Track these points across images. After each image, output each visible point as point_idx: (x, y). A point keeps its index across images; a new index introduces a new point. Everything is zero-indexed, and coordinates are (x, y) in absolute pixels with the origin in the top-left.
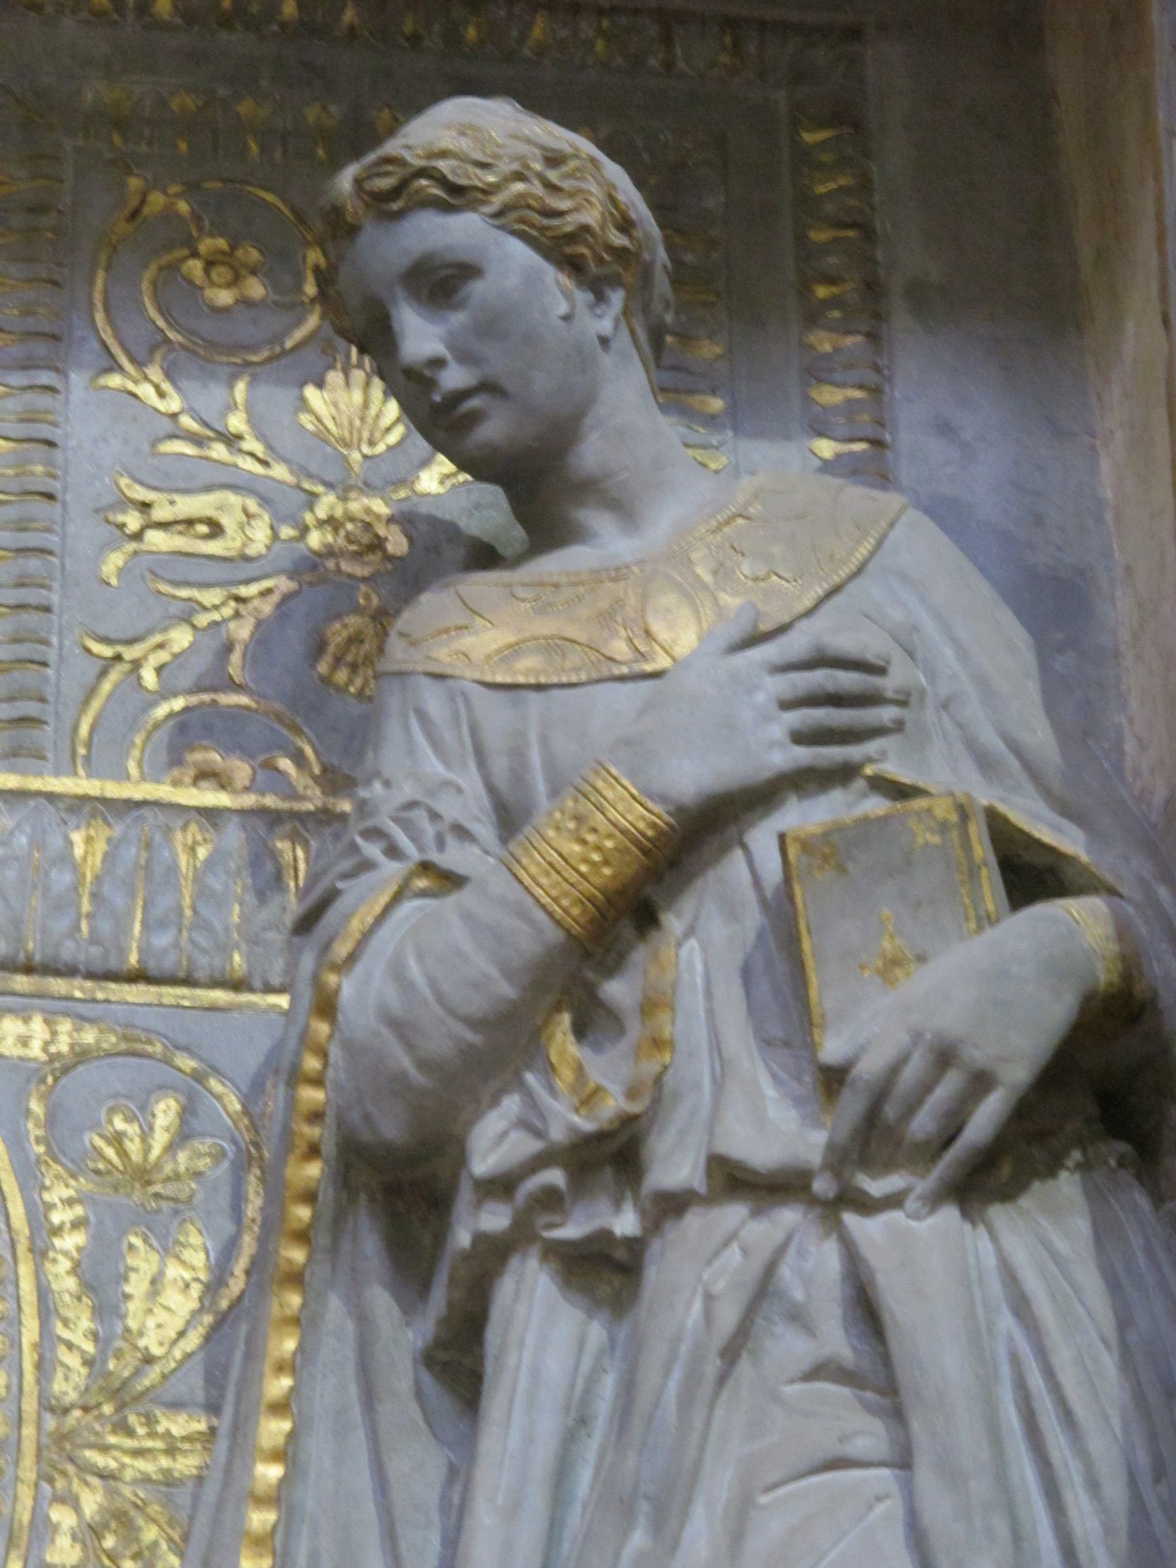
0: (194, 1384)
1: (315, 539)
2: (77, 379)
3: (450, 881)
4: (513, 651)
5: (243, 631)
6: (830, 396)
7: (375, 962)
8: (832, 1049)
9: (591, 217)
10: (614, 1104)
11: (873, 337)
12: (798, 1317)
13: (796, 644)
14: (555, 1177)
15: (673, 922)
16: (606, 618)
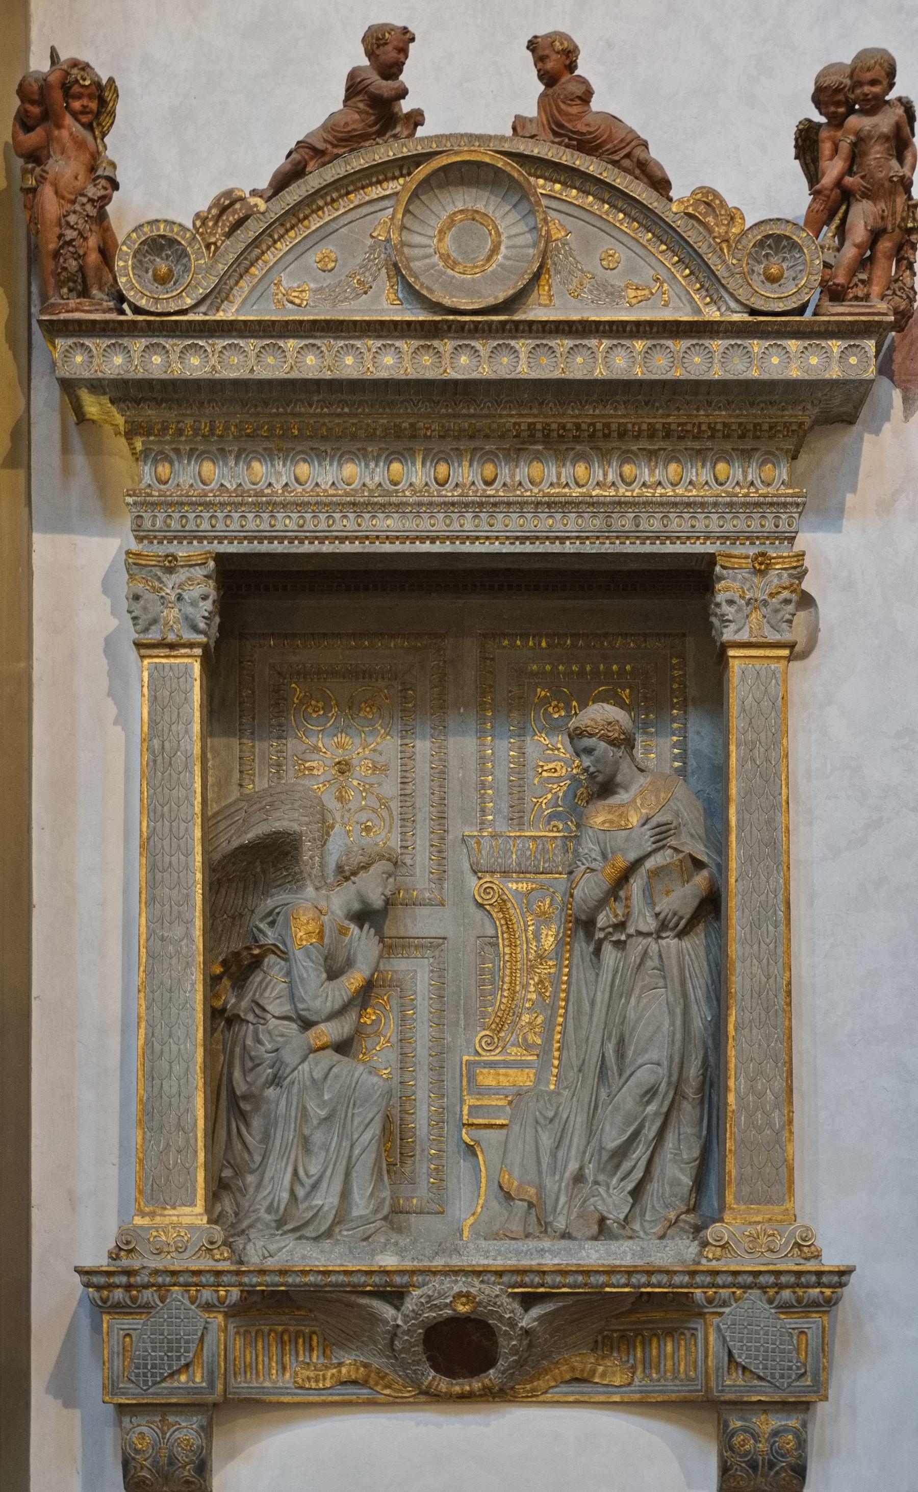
0: (553, 955)
1: (575, 771)
2: (528, 738)
3: (593, 870)
4: (604, 822)
5: (561, 794)
6: (675, 725)
7: (579, 888)
8: (657, 909)
9: (616, 735)
10: (621, 918)
11: (685, 712)
12: (651, 958)
13: (653, 822)
14: (610, 930)
15: (632, 881)
16: (620, 816)
